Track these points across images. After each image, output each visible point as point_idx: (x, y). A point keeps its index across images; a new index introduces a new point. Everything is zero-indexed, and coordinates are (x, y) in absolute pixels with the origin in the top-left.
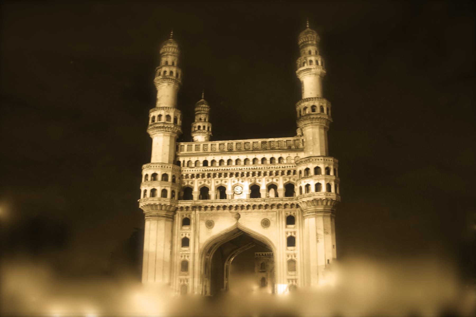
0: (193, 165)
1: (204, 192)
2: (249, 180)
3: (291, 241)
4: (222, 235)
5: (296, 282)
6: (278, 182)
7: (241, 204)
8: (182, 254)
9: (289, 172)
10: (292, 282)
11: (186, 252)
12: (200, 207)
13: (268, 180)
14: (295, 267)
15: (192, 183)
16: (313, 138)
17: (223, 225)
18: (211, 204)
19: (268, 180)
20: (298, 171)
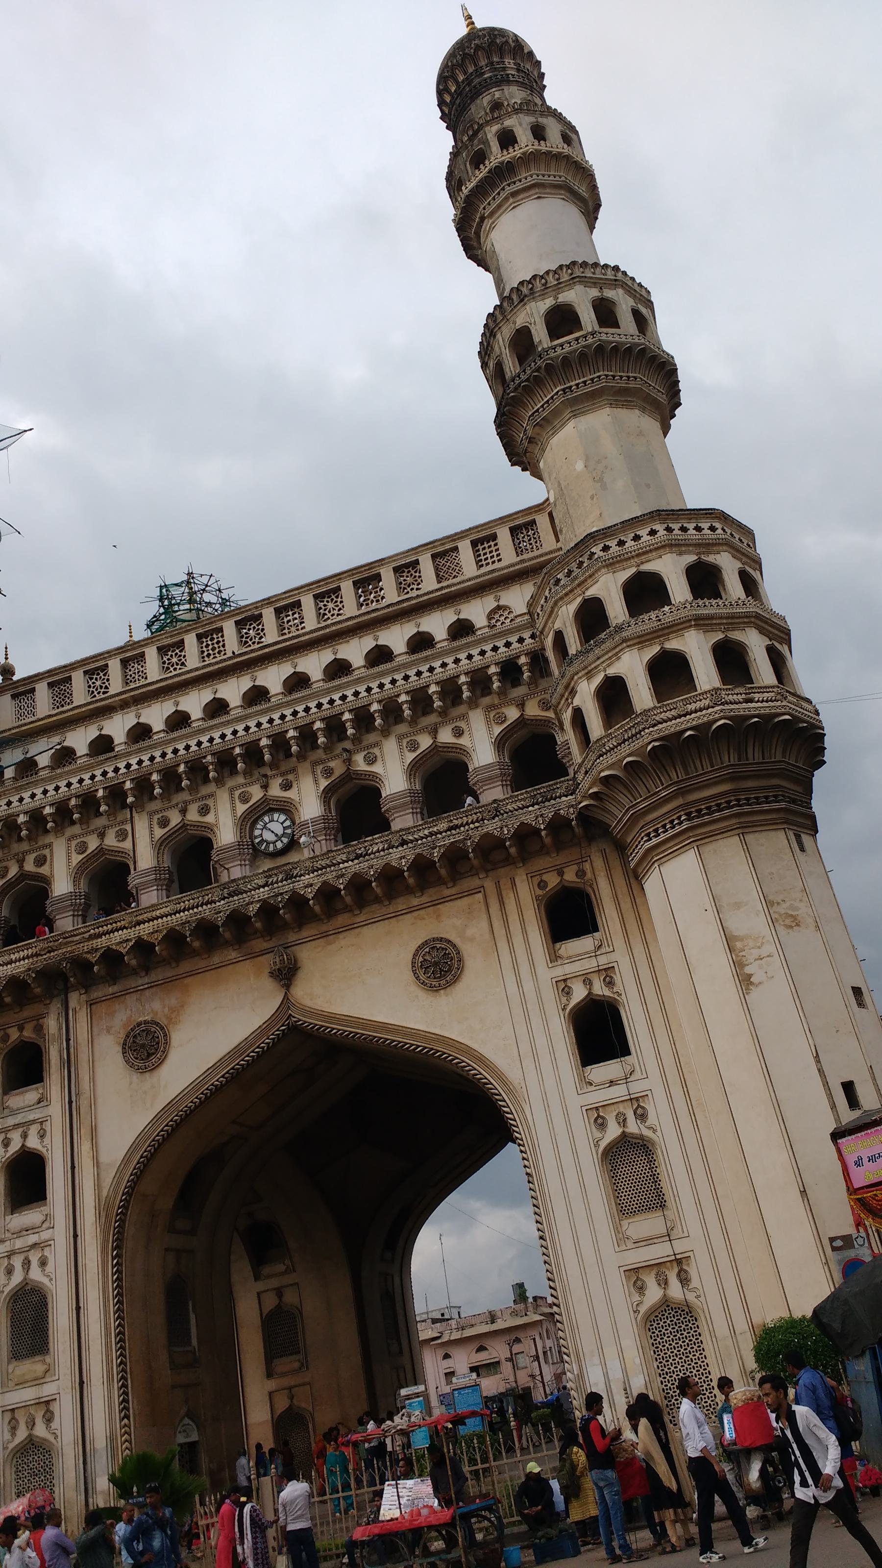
3: (599, 1032)
4: (217, 1090)
5: (684, 1279)
6: (464, 741)
7: (286, 887)
8: (11, 1254)
9: (510, 671)
10: (664, 1283)
11: (33, 1239)
14: (655, 1179)
16: (587, 459)
17: (218, 1025)
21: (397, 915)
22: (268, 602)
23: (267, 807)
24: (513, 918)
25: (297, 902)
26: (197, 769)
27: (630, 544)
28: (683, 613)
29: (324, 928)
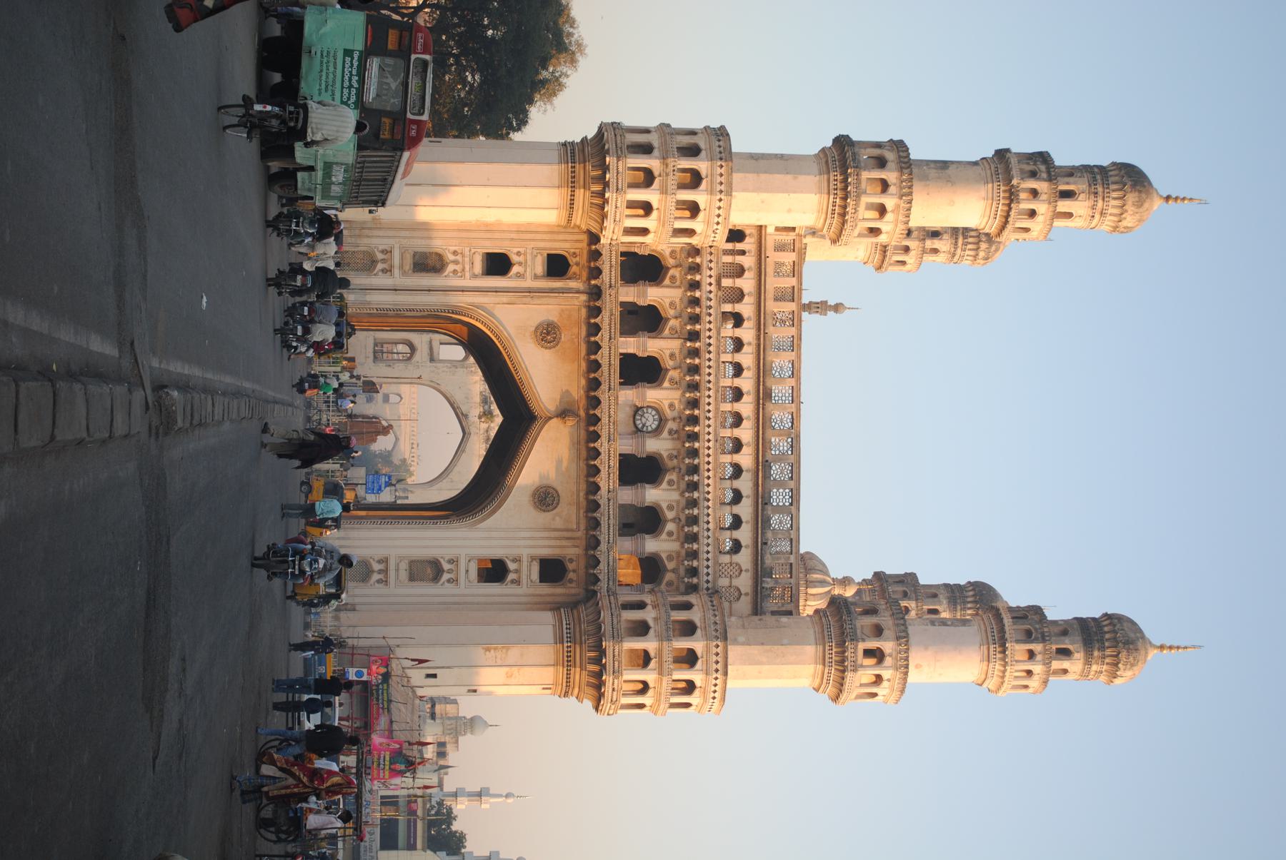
0: (727, 282)
1: (645, 320)
2: (675, 453)
5: (379, 581)
6: (664, 536)
7: (604, 434)
8: (463, 256)
9: (694, 572)
10: (380, 572)
12: (595, 311)
13: (670, 508)
15: (673, 277)
17: (546, 376)
18: (605, 345)
19: (670, 508)
20: (692, 598)
21: (578, 483)
22: (798, 436)
23: (662, 421)
24: (558, 543)
25: (595, 436)
26: (694, 387)
27: (715, 658)
28: (665, 672)
29: (583, 442)
